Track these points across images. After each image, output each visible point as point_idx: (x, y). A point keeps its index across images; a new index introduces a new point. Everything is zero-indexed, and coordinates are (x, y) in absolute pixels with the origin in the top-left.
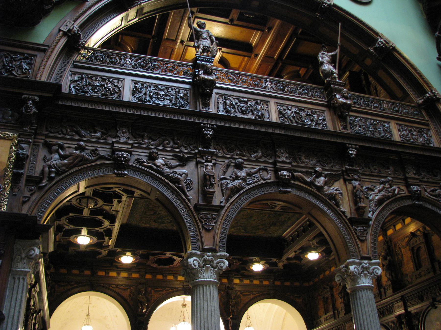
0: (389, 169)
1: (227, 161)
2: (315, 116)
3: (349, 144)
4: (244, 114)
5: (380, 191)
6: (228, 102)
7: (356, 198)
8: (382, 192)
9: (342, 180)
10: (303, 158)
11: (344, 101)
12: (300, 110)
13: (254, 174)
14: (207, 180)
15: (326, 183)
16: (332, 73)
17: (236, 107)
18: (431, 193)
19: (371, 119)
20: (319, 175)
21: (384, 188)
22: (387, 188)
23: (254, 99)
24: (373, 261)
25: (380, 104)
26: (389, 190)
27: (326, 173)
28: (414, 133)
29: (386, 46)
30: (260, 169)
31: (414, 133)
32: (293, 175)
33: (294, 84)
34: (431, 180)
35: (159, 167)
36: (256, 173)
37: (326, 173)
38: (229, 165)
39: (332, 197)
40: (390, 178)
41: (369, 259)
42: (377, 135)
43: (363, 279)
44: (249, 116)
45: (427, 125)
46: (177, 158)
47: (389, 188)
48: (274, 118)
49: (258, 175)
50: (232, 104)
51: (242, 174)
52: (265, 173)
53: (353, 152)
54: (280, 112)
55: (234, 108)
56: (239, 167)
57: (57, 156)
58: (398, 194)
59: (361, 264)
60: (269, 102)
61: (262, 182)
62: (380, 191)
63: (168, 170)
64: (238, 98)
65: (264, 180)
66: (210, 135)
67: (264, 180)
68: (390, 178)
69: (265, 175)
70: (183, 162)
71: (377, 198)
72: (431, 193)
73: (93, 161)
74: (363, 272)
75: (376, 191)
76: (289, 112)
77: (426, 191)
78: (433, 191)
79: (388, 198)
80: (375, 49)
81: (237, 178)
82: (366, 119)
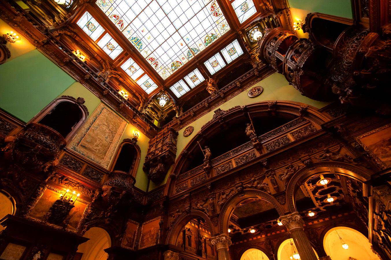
0: (289, 159)
1: (218, 194)
2: (250, 155)
3: (262, 161)
4: (224, 171)
5: (287, 174)
6: (217, 170)
7: (274, 183)
8: (289, 173)
9: (266, 178)
10: (246, 177)
11: (255, 143)
12: (244, 156)
13: (229, 194)
14: (213, 205)
15: (258, 183)
16: (252, 133)
17: (221, 170)
18: (320, 158)
19: (276, 140)
20: (254, 181)
21: (288, 171)
22: (290, 170)
23: (226, 163)
24: (293, 213)
25: (280, 129)
26: (292, 170)
27: (257, 178)
28: (302, 132)
29: (272, 105)
30: (231, 191)
31: (302, 132)
32: (243, 187)
33: (240, 147)
34: (317, 151)
35: (198, 207)
36: (230, 193)
37: (257, 178)
38: (220, 195)
39: (262, 189)
40: (290, 164)
41: (290, 213)
42: (281, 146)
43: (292, 225)
44: (226, 171)
45: (310, 122)
46: (204, 201)
47: (291, 169)
48: (235, 166)
49: (231, 194)
50: (219, 170)
51: (225, 196)
52: (233, 191)
53: (265, 163)
54: (236, 162)
55: (220, 171)
56: (223, 194)
57: (172, 218)
58: (298, 169)
59: (286, 217)
60: (231, 161)
61: (233, 195)
62: (287, 174)
63: (202, 207)
64: (220, 166)
65: (233, 194)
66: (210, 188)
67: (233, 194)
68: (290, 164)
69: (233, 192)
70: (205, 201)
71: (285, 178)
72: (320, 158)
73: (181, 214)
74: (289, 221)
75: (285, 174)
76: (239, 160)
77: (316, 159)
78: (321, 156)
79: (293, 174)
80: (270, 108)
81: (223, 199)
82: (273, 142)
